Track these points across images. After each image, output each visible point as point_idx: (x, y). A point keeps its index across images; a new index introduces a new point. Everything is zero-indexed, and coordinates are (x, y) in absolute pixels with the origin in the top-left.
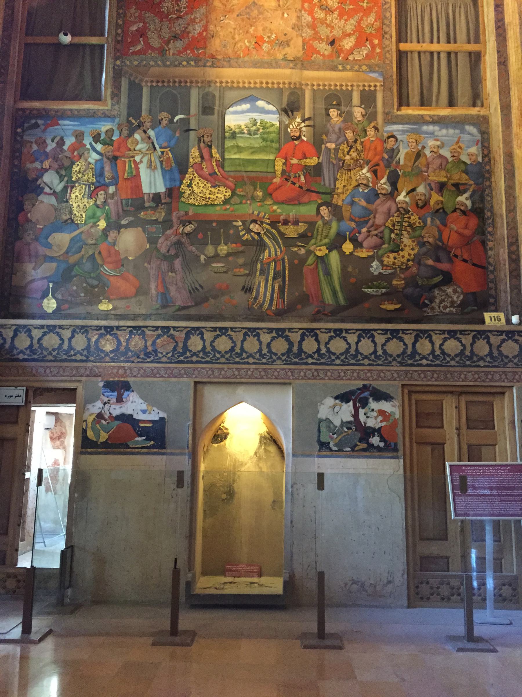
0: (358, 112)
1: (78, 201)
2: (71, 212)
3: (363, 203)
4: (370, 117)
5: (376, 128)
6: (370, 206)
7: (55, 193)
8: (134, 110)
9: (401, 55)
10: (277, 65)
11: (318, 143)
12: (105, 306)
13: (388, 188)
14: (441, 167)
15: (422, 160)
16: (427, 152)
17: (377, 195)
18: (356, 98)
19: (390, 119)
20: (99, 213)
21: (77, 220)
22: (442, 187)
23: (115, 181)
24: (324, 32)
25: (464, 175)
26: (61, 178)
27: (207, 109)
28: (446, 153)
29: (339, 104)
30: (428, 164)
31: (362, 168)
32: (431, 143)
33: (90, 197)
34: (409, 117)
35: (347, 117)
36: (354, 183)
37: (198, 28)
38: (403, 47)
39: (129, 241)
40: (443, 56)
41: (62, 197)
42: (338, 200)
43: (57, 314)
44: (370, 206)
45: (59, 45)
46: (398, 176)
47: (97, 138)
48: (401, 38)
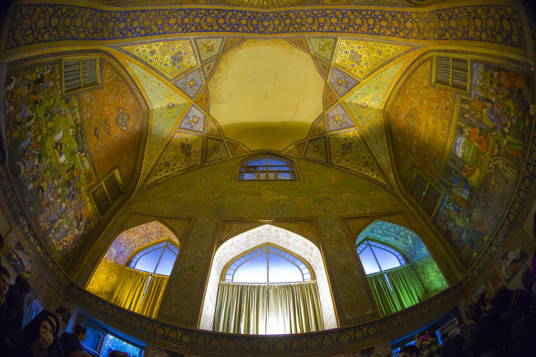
0: (467, 107)
1: (459, 222)
2: (460, 227)
3: (494, 116)
4: (468, 102)
5: (472, 101)
6: (495, 114)
7: (454, 227)
8: (447, 186)
9: (453, 86)
10: (449, 130)
11: (473, 126)
12: (486, 238)
13: (490, 104)
14: (485, 80)
15: (483, 87)
16: (481, 84)
17: (492, 109)
18: (462, 106)
19: (470, 96)
20: (464, 218)
21: (463, 227)
22: (491, 82)
23: (460, 206)
24: (443, 111)
25: (488, 72)
26: (451, 222)
27: (454, 162)
28: (481, 77)
29: (463, 113)
30: (484, 85)
31: (483, 112)
32: (478, 82)
33: (460, 217)
34: (470, 88)
35: (468, 111)
36: (487, 117)
37: (434, 152)
38: (450, 84)
39: (476, 214)
40: (454, 71)
41: (456, 226)
42: (491, 126)
43: (478, 255)
44: (495, 114)
45: (425, 197)
46: (487, 98)
47: (448, 203)
48: (448, 85)
